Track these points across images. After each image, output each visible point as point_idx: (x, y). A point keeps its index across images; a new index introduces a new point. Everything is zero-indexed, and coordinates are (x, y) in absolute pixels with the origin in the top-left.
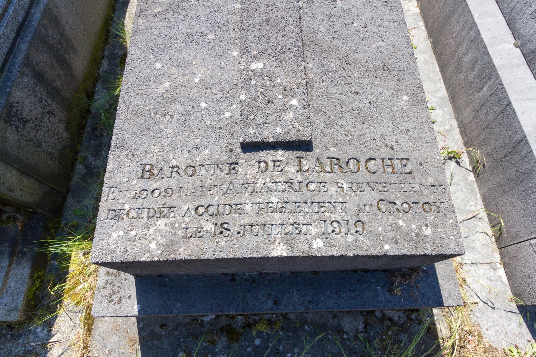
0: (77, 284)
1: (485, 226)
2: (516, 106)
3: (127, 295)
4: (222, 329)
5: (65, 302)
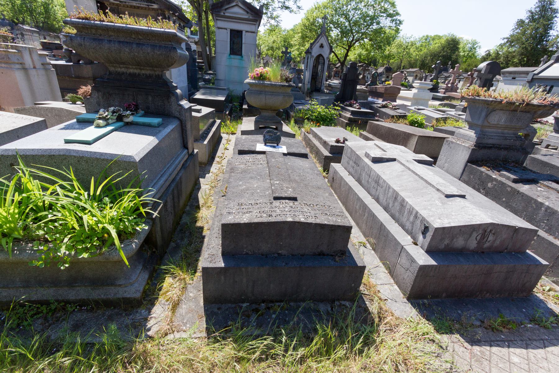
0: (167, 291)
1: (383, 269)
2: (376, 214)
3: (219, 260)
4: (253, 310)
5: (160, 299)
